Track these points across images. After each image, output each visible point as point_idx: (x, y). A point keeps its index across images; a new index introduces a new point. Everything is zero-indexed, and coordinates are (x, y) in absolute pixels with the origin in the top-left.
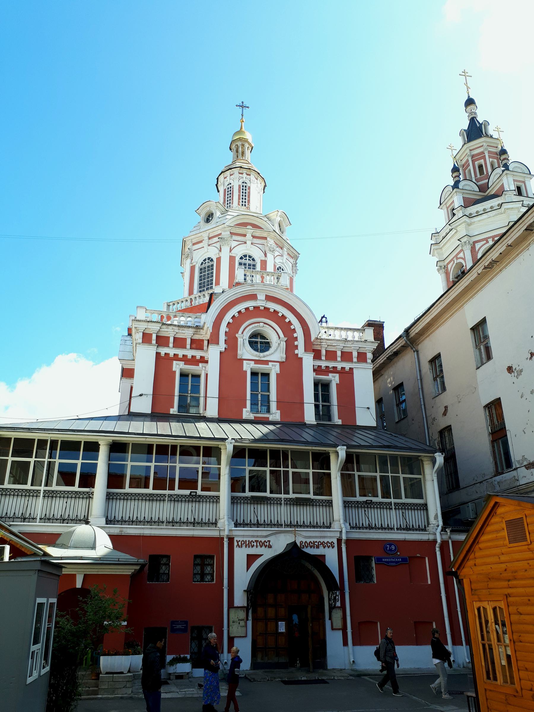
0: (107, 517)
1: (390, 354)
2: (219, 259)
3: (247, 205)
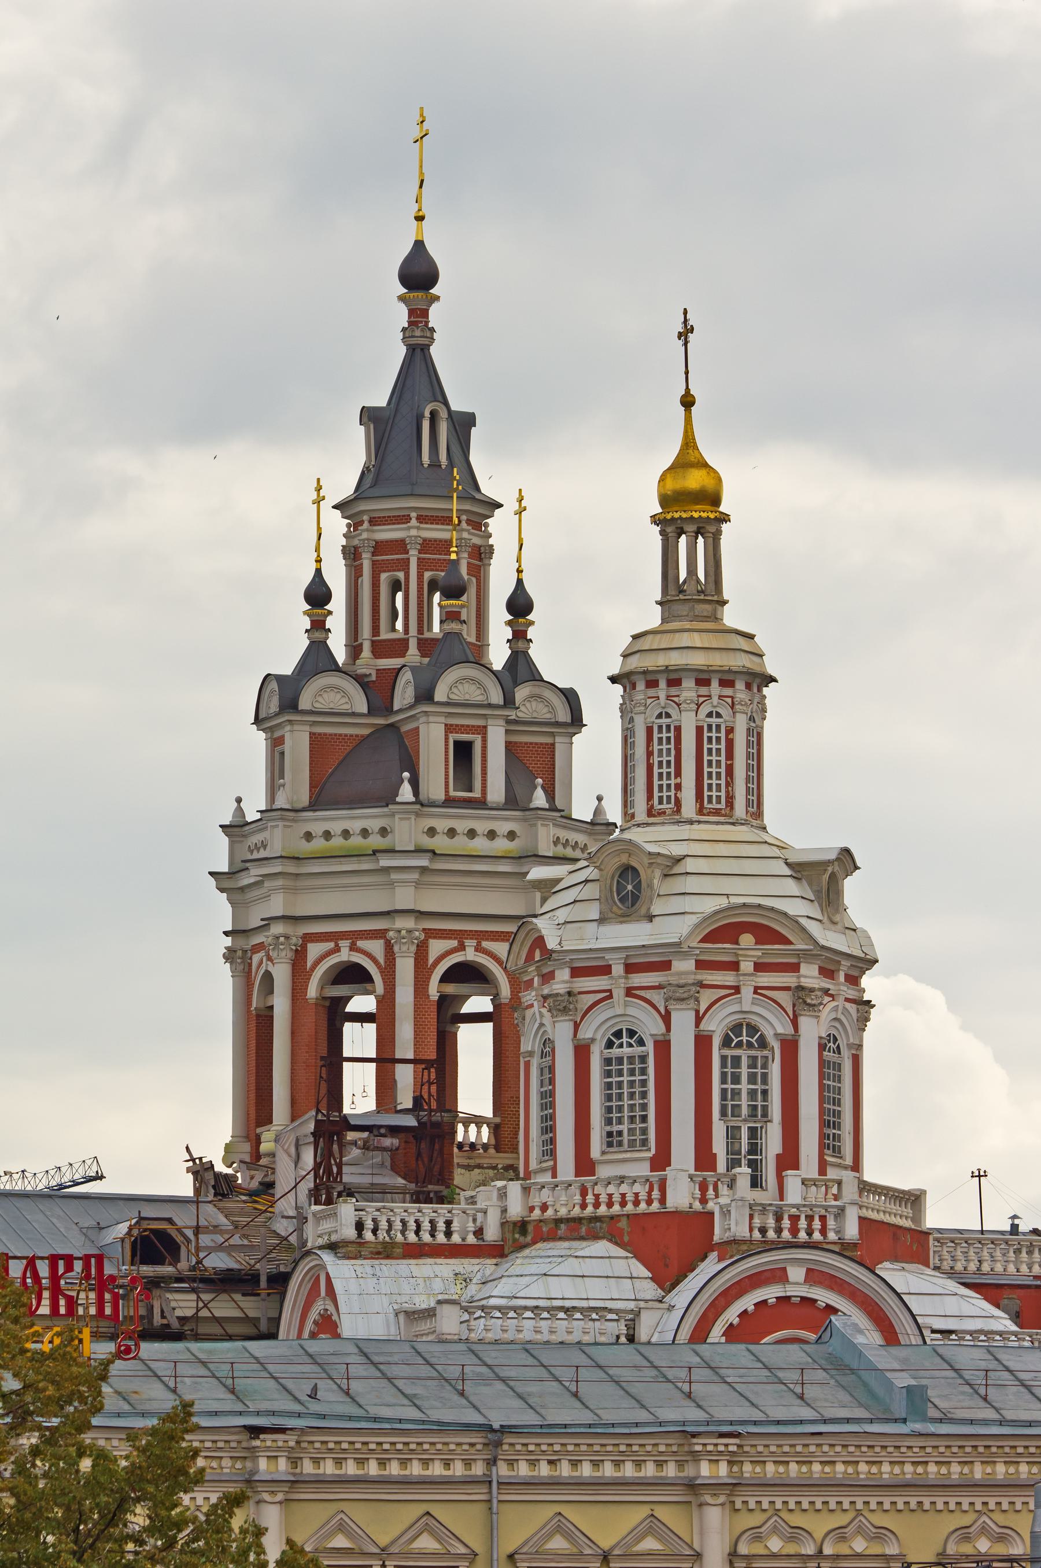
2: (663, 1047)
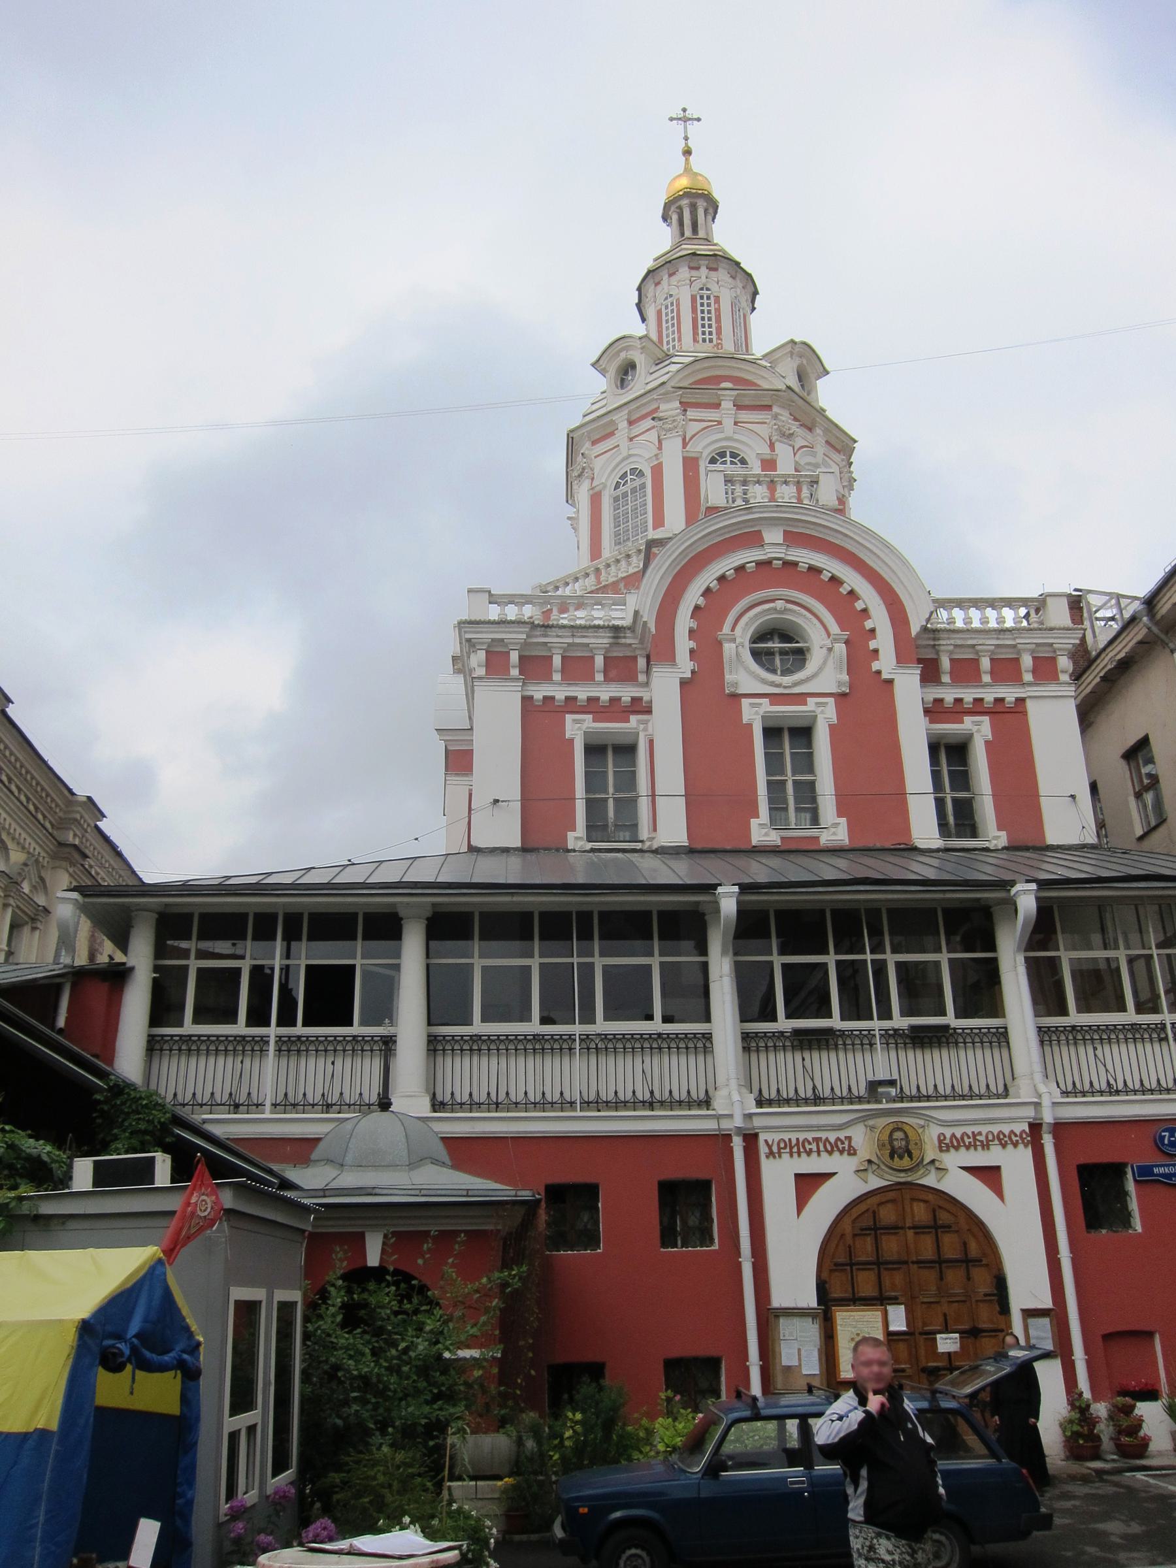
0: (434, 1094)
1: (1109, 667)
2: (657, 471)
3: (714, 340)
